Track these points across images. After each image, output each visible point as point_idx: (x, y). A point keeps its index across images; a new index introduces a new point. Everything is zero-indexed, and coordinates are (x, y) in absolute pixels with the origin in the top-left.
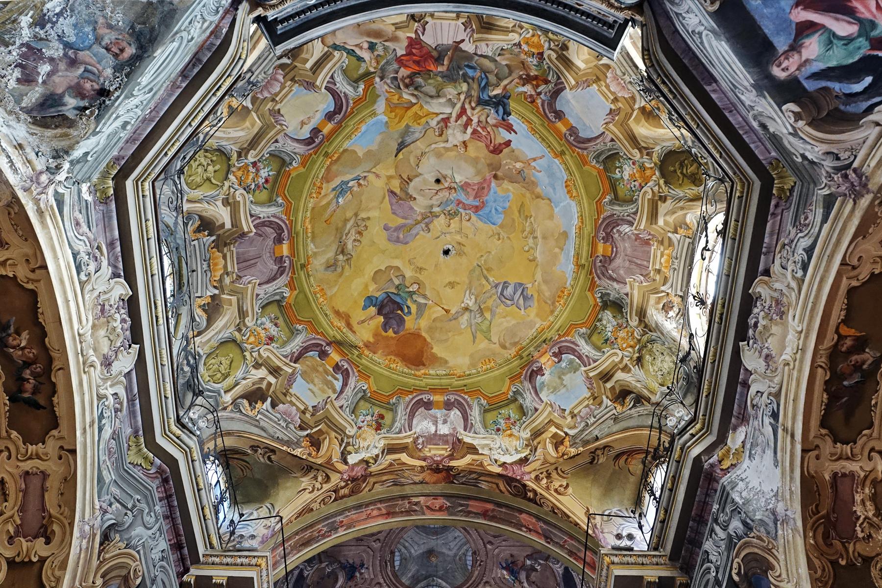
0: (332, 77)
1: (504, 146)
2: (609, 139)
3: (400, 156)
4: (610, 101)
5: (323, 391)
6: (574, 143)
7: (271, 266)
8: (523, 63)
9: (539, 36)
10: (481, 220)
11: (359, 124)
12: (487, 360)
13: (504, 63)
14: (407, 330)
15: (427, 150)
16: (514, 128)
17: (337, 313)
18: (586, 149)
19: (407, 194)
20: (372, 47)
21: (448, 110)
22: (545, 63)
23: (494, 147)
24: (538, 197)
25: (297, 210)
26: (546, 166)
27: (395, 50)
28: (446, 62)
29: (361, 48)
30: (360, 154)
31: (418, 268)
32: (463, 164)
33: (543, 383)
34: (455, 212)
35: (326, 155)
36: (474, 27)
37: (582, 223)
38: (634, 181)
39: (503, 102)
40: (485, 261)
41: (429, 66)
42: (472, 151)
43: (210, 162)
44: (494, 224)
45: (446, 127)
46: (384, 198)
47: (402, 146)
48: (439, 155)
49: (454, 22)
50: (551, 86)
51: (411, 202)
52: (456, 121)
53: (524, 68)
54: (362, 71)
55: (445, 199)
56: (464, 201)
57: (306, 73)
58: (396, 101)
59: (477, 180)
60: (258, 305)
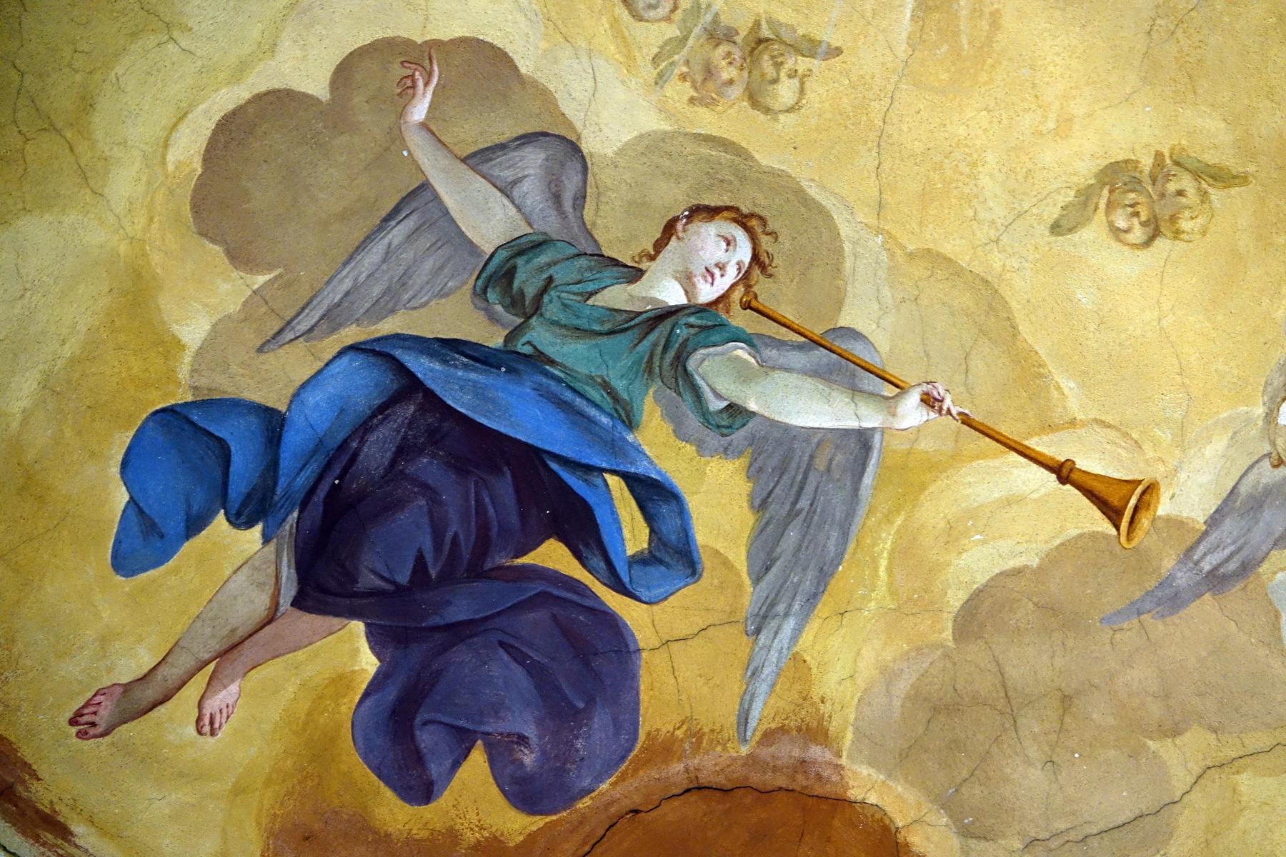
14: (664, 749)
31: (718, 35)
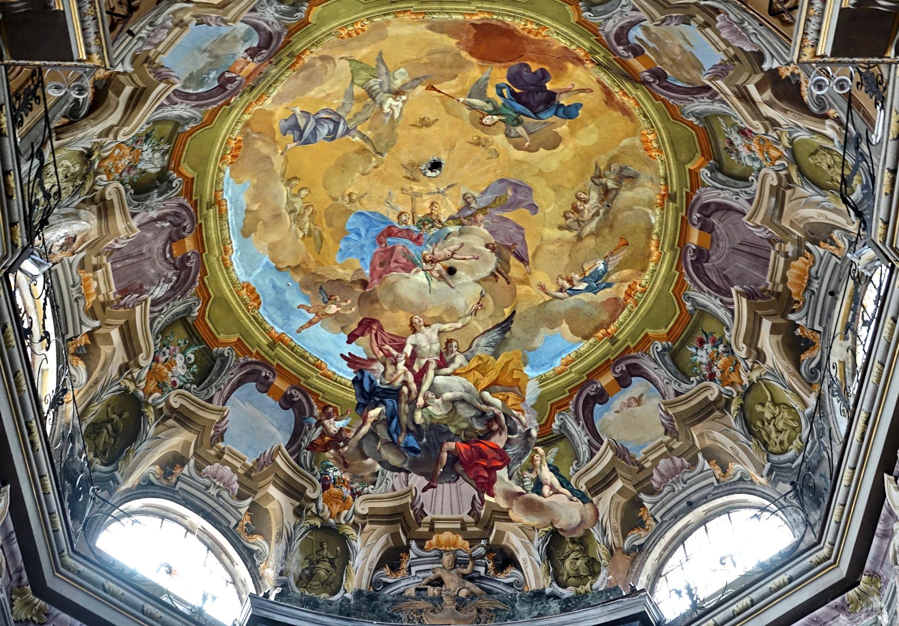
0: (592, 455)
1: (357, 333)
2: (215, 401)
3: (507, 312)
4: (227, 451)
5: (668, 35)
6: (259, 367)
7: (720, 226)
8: (345, 466)
9: (331, 517)
10: (382, 216)
11: (563, 371)
12: (354, 35)
13: (370, 461)
14: (504, 67)
15: (469, 318)
16: (346, 363)
17: (626, 112)
18: (243, 366)
19: (499, 255)
20: (538, 486)
21: (440, 380)
22: (319, 476)
23: (371, 328)
24: (296, 269)
25: (668, 279)
26: (292, 318)
27: (510, 478)
28: (445, 455)
29: (552, 487)
30: (565, 326)
31: (484, 146)
32: (413, 297)
33: (246, 41)
34: (424, 225)
35: (613, 340)
36: (412, 512)
37: (224, 260)
38: (166, 360)
39: (365, 398)
40: (371, 162)
41: (466, 450)
42: (402, 318)
43: (766, 423)
44: (361, 214)
45: (441, 355)
46: (534, 255)
47: (505, 326)
48: (451, 312)
49: (437, 516)
50: (306, 442)
51: (493, 241)
52: (427, 362)
53: (343, 457)
54: (554, 450)
55: (439, 244)
56: (410, 243)
57: (624, 474)
58: (511, 395)
59: (392, 277)
60: (753, 188)
